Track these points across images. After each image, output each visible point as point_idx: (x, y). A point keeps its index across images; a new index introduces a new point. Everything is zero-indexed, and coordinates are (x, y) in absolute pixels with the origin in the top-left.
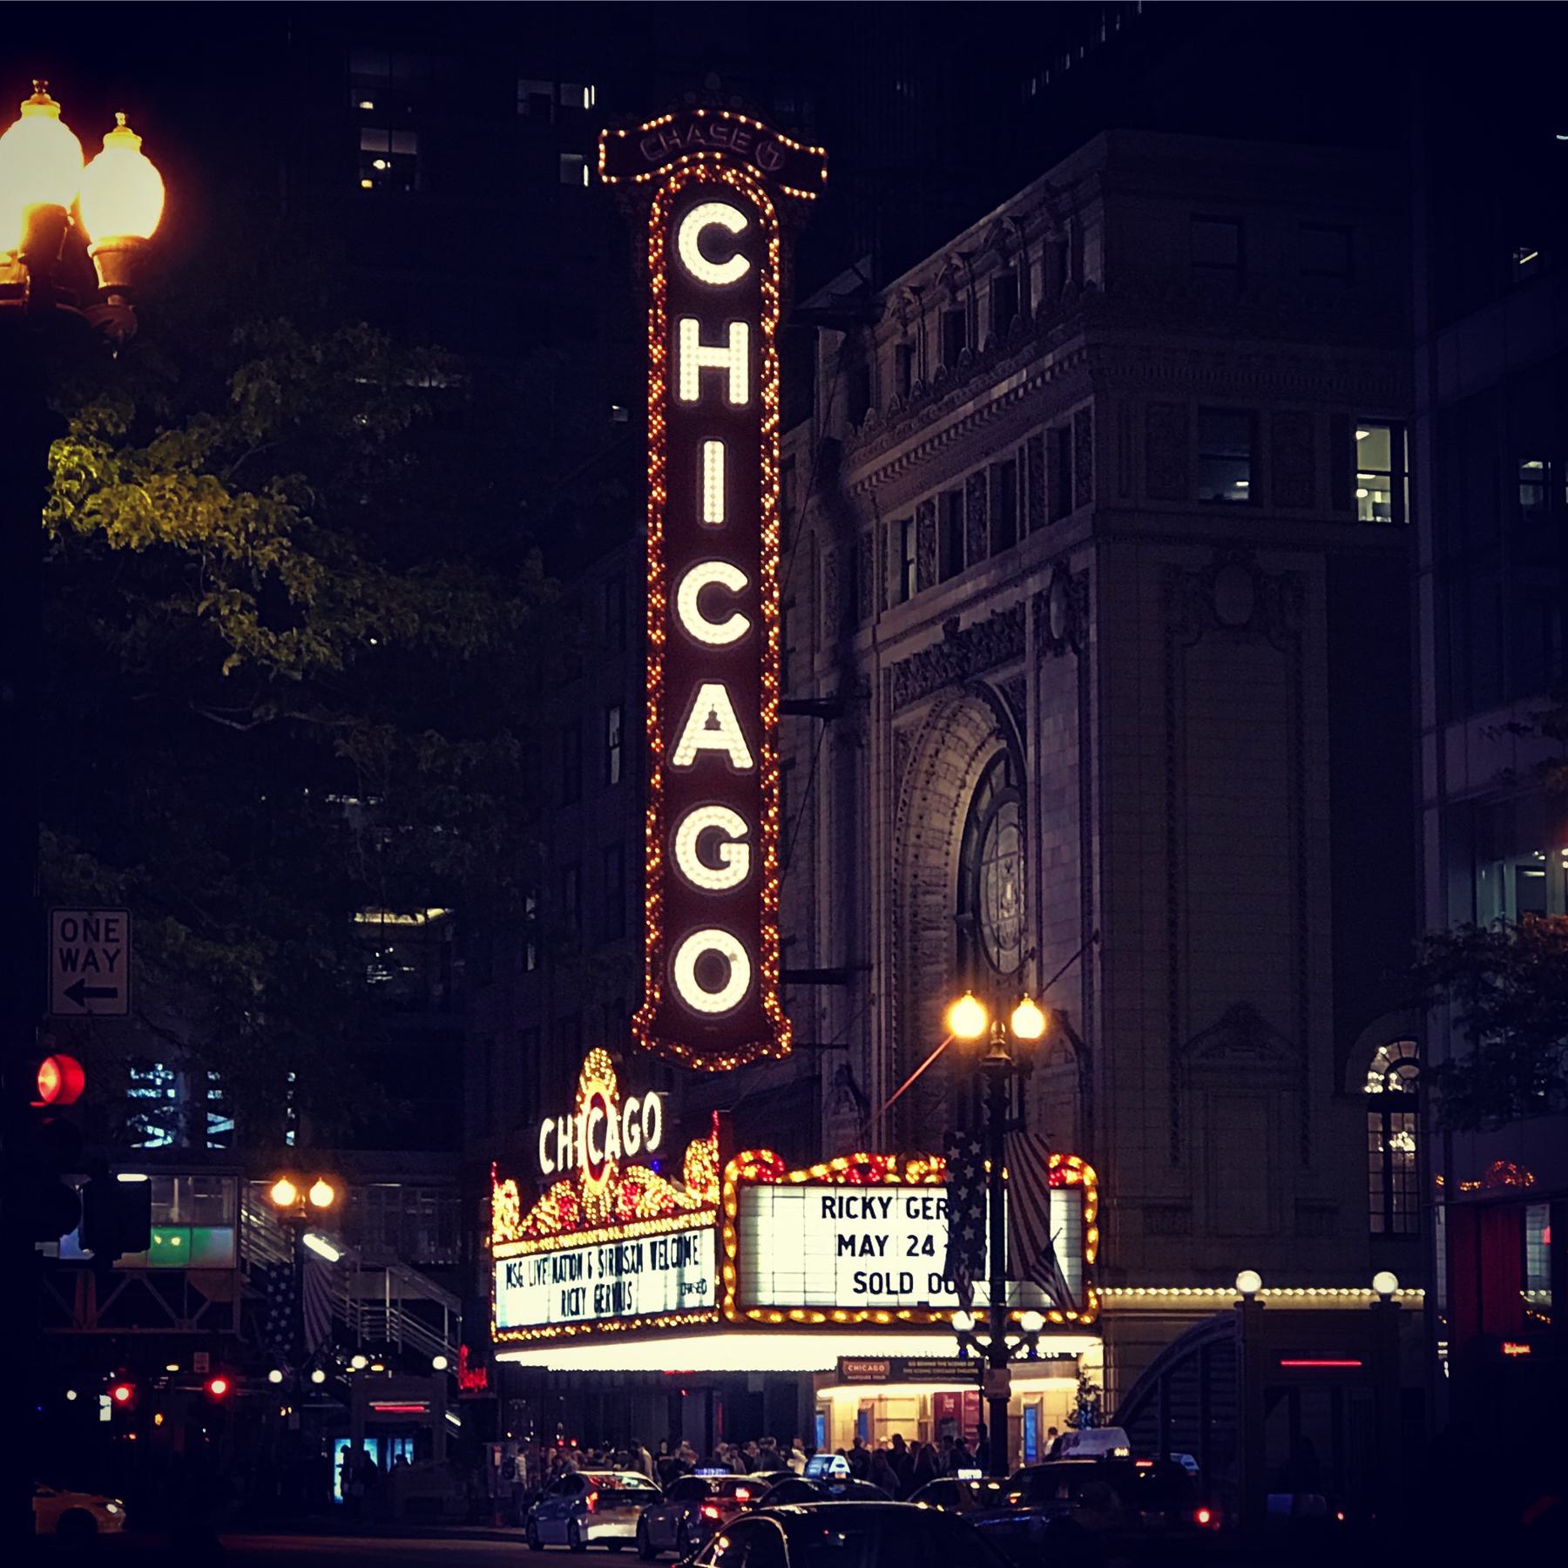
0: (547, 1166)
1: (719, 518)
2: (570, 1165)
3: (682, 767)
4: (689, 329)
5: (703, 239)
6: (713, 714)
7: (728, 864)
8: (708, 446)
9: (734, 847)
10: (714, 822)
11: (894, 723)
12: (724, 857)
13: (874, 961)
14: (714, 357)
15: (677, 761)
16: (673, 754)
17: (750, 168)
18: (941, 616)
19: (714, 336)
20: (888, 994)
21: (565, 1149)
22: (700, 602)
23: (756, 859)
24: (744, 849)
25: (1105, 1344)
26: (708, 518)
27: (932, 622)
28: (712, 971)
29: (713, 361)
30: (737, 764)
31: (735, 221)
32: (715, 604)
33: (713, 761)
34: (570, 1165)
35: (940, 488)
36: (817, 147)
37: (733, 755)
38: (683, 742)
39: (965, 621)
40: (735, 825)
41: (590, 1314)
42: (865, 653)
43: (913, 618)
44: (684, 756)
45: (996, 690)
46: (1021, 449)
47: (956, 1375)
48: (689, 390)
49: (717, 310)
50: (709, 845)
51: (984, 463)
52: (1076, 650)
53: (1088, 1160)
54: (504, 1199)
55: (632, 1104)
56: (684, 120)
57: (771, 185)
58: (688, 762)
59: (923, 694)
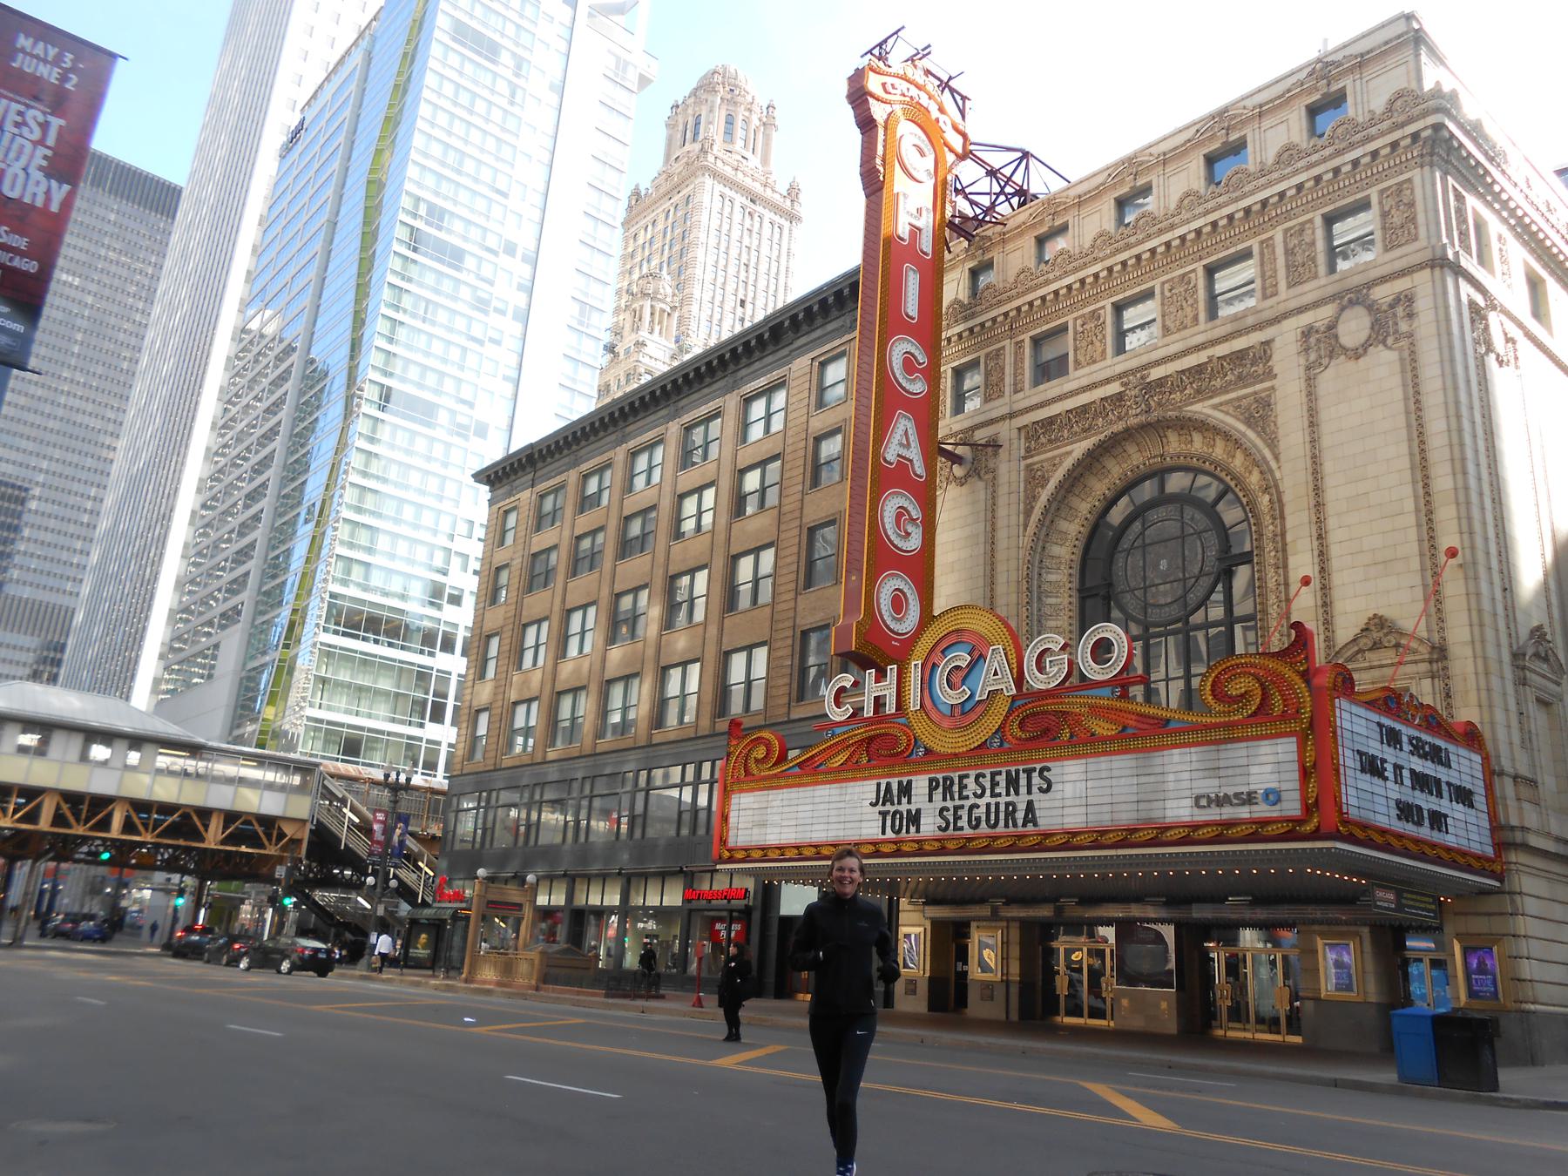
2: (890, 708)
7: (908, 534)
27: (1108, 381)
33: (903, 465)
34: (890, 708)
39: (1156, 373)
52: (1390, 348)
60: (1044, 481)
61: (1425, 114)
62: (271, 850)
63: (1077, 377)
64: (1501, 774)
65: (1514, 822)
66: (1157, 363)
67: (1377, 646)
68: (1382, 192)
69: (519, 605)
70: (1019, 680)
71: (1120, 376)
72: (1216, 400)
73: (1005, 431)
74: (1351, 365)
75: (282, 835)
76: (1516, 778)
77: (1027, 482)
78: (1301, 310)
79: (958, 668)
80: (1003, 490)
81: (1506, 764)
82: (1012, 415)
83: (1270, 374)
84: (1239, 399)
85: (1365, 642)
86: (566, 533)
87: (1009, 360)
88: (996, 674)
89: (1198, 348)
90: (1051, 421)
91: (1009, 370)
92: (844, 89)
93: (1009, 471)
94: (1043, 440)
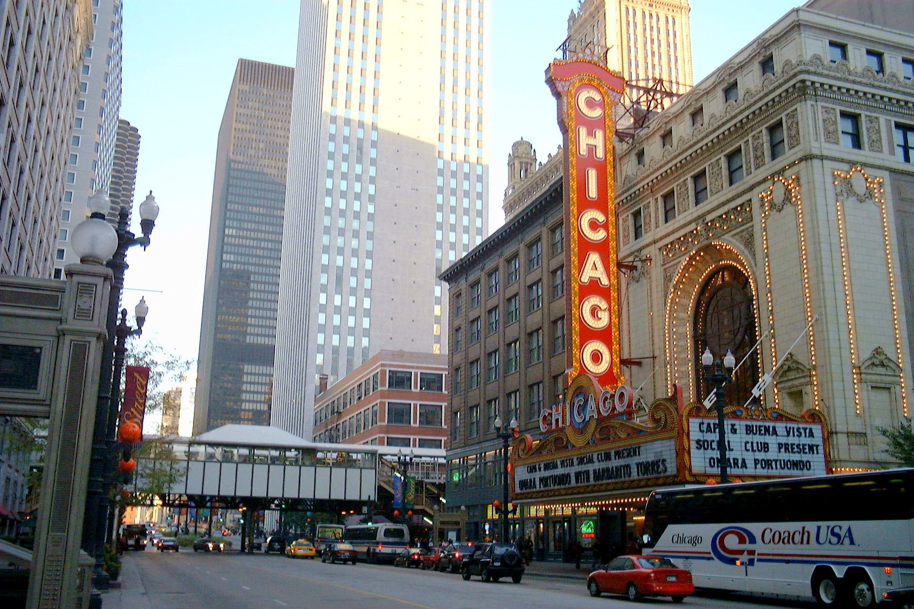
14: (592, 141)
19: (591, 134)
27: (690, 223)
28: (596, 357)
32: (594, 225)
33: (594, 282)
39: (709, 218)
43: (677, 225)
44: (585, 279)
48: (583, 151)
50: (594, 311)
51: (722, 155)
61: (795, 75)
63: (680, 219)
64: (836, 433)
65: (842, 457)
66: (709, 212)
67: (789, 369)
68: (787, 115)
69: (467, 349)
71: (696, 220)
73: (652, 251)
74: (778, 214)
76: (848, 434)
77: (665, 279)
80: (654, 284)
81: (840, 427)
82: (655, 242)
84: (742, 232)
85: (786, 368)
86: (483, 309)
87: (652, 209)
89: (723, 204)
91: (653, 215)
92: (543, 77)
93: (656, 271)
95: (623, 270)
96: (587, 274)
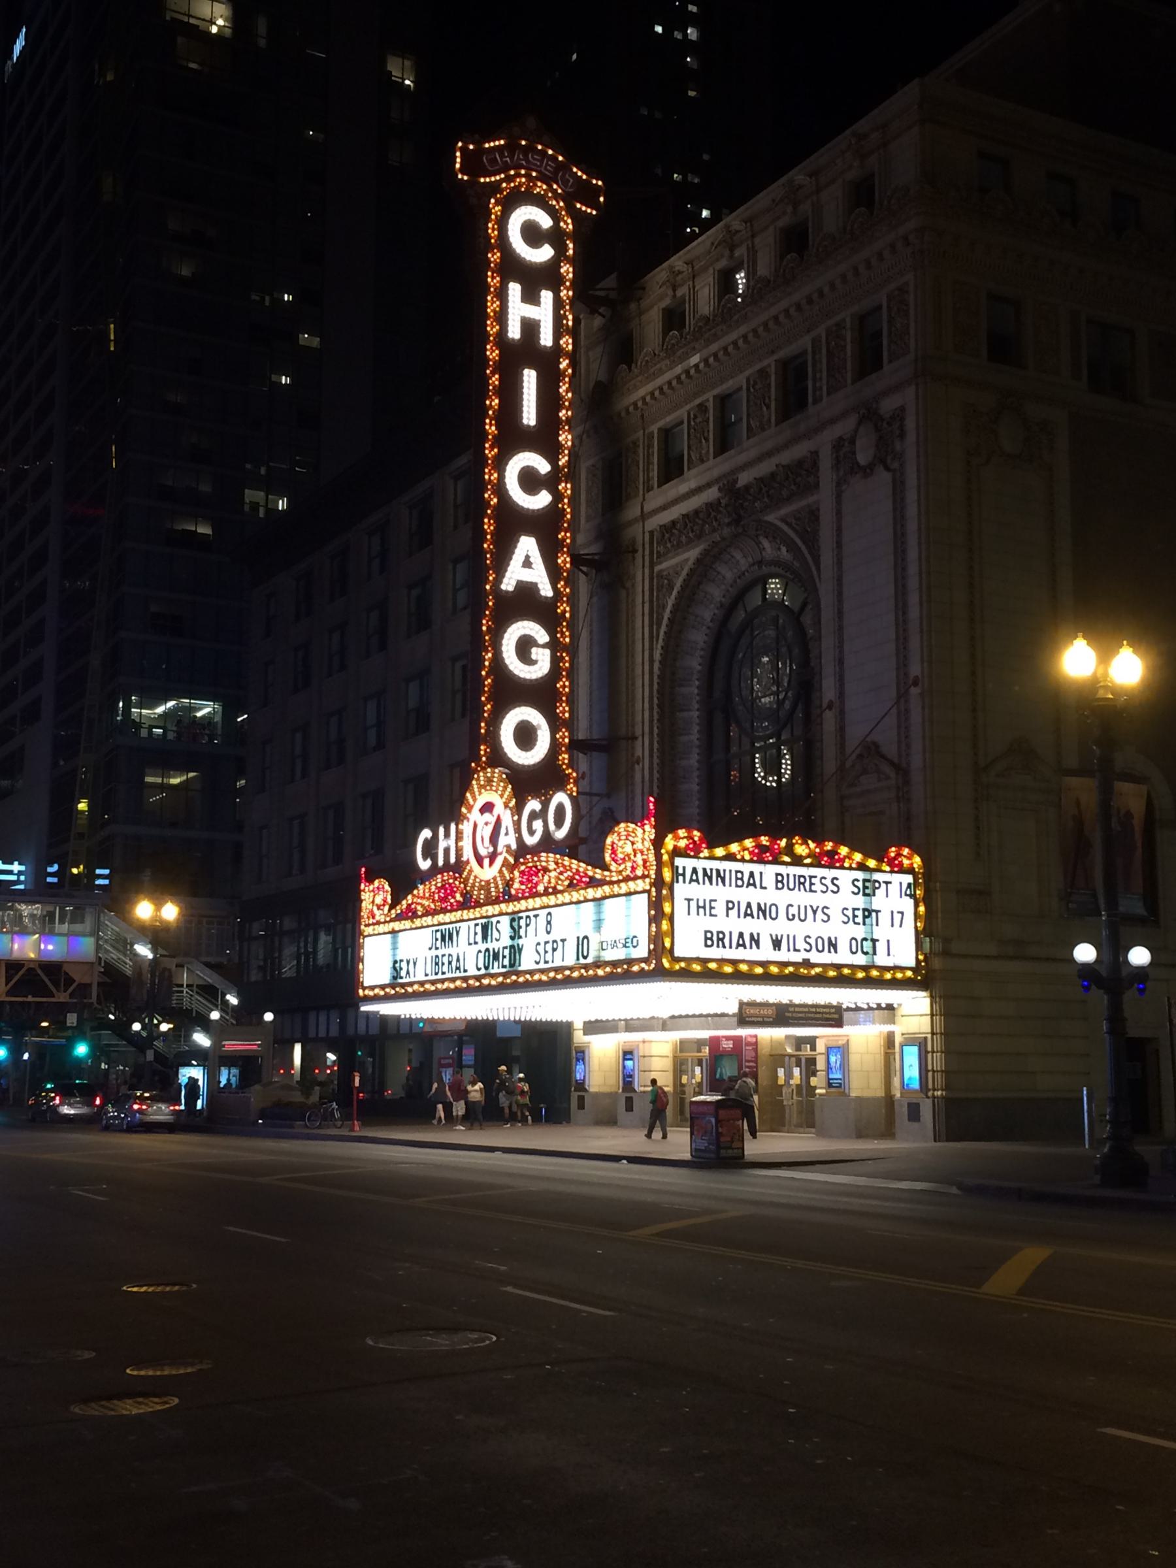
0: (424, 865)
1: (533, 422)
2: (453, 860)
3: (507, 592)
4: (515, 290)
5: (525, 227)
6: (527, 557)
8: (526, 372)
9: (540, 650)
10: (528, 632)
11: (657, 568)
12: (534, 657)
13: (638, 732)
14: (530, 311)
15: (503, 587)
16: (501, 582)
17: (555, 186)
18: (717, 481)
19: (530, 297)
20: (651, 756)
21: (447, 851)
22: (520, 478)
23: (555, 661)
24: (547, 652)
25: (932, 997)
26: (525, 421)
27: (708, 485)
28: (525, 737)
29: (528, 314)
30: (543, 593)
31: (546, 222)
33: (526, 590)
34: (453, 860)
35: (716, 392)
36: (597, 180)
37: (540, 586)
38: (508, 574)
39: (744, 479)
40: (542, 636)
41: (570, 960)
42: (631, 523)
45: (779, 523)
46: (815, 342)
47: (821, 1019)
48: (514, 332)
49: (535, 280)
50: (525, 647)
52: (887, 469)
53: (915, 850)
54: (374, 896)
55: (533, 805)
56: (512, 146)
57: (569, 199)
58: (511, 588)
59: (690, 541)
60: (671, 587)
62: (62, 997)
70: (520, 840)
72: (783, 511)
75: (70, 981)
78: (833, 421)
79: (486, 824)
83: (817, 486)
88: (507, 834)
89: (769, 454)
90: (674, 523)
94: (669, 545)
95: (584, 569)
96: (513, 576)
